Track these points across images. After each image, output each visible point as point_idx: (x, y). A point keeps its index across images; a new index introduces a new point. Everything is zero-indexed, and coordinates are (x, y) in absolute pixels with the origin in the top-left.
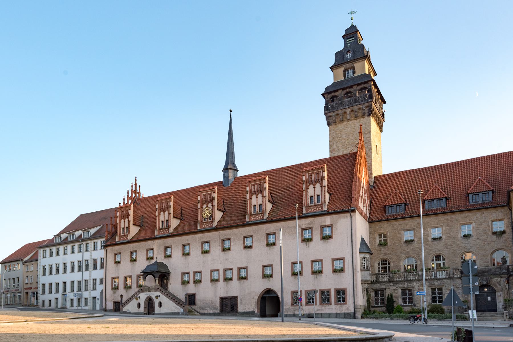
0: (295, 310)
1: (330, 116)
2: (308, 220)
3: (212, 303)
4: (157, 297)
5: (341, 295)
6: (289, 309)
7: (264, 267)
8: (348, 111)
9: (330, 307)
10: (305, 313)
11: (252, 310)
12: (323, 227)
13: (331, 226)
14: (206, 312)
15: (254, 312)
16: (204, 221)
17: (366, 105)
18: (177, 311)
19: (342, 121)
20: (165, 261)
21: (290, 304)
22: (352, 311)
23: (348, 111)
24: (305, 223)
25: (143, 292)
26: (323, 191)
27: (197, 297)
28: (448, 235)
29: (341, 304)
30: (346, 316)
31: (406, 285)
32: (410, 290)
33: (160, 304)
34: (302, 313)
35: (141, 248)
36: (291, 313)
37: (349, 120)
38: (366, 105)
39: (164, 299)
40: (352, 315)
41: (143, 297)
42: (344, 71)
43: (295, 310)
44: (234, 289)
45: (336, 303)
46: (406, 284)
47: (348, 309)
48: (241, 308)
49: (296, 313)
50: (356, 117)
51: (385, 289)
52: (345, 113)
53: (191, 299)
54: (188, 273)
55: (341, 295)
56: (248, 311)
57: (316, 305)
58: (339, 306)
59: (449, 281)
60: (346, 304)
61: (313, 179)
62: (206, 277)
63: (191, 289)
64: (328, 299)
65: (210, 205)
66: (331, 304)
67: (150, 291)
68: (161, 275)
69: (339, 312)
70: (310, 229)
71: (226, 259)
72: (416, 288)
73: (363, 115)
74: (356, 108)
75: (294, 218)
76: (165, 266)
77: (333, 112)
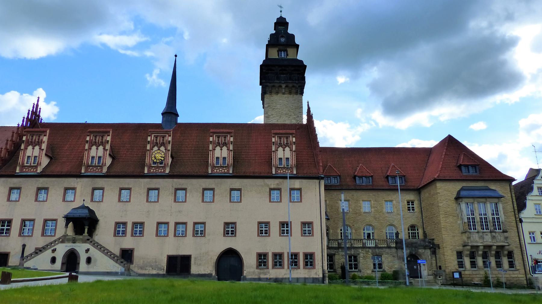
0: (260, 273)
1: (267, 86)
2: (277, 181)
3: (156, 262)
4: (87, 251)
5: (309, 259)
6: (254, 272)
7: (227, 224)
8: (284, 86)
9: (299, 271)
10: (271, 277)
11: (209, 272)
12: (292, 189)
13: (300, 189)
14: (146, 272)
15: (212, 274)
16: (153, 165)
17: (299, 85)
18: (114, 270)
19: (277, 93)
20: (92, 206)
21: (255, 266)
22: (321, 276)
23: (284, 86)
24: (273, 183)
25: (63, 242)
26: (229, 155)
27: (136, 254)
28: (376, 209)
29: (309, 269)
30: (315, 280)
31: (353, 252)
32: (355, 257)
33: (89, 260)
34: (268, 276)
35: (57, 186)
36: (256, 277)
37: (284, 94)
38: (299, 85)
39: (94, 253)
40: (321, 279)
41: (62, 249)
42: (278, 51)
43: (260, 273)
44: (185, 246)
45: (304, 268)
46: (353, 250)
47: (316, 274)
48: (194, 269)
49: (262, 276)
50: (290, 93)
51: (335, 254)
52: (281, 86)
53: (127, 256)
54: (125, 224)
55: (309, 259)
56: (203, 272)
57: (283, 268)
58: (307, 270)
59: (388, 250)
60: (315, 268)
61: (220, 141)
62: (150, 229)
63: (128, 242)
64: (296, 262)
65: (162, 148)
66: (299, 268)
67: (74, 243)
68: (84, 223)
69: (307, 276)
70: (279, 189)
71: (180, 212)
72: (361, 255)
73: (296, 93)
74: (290, 85)
75: (285, 178)
76: (92, 212)
77: (270, 83)
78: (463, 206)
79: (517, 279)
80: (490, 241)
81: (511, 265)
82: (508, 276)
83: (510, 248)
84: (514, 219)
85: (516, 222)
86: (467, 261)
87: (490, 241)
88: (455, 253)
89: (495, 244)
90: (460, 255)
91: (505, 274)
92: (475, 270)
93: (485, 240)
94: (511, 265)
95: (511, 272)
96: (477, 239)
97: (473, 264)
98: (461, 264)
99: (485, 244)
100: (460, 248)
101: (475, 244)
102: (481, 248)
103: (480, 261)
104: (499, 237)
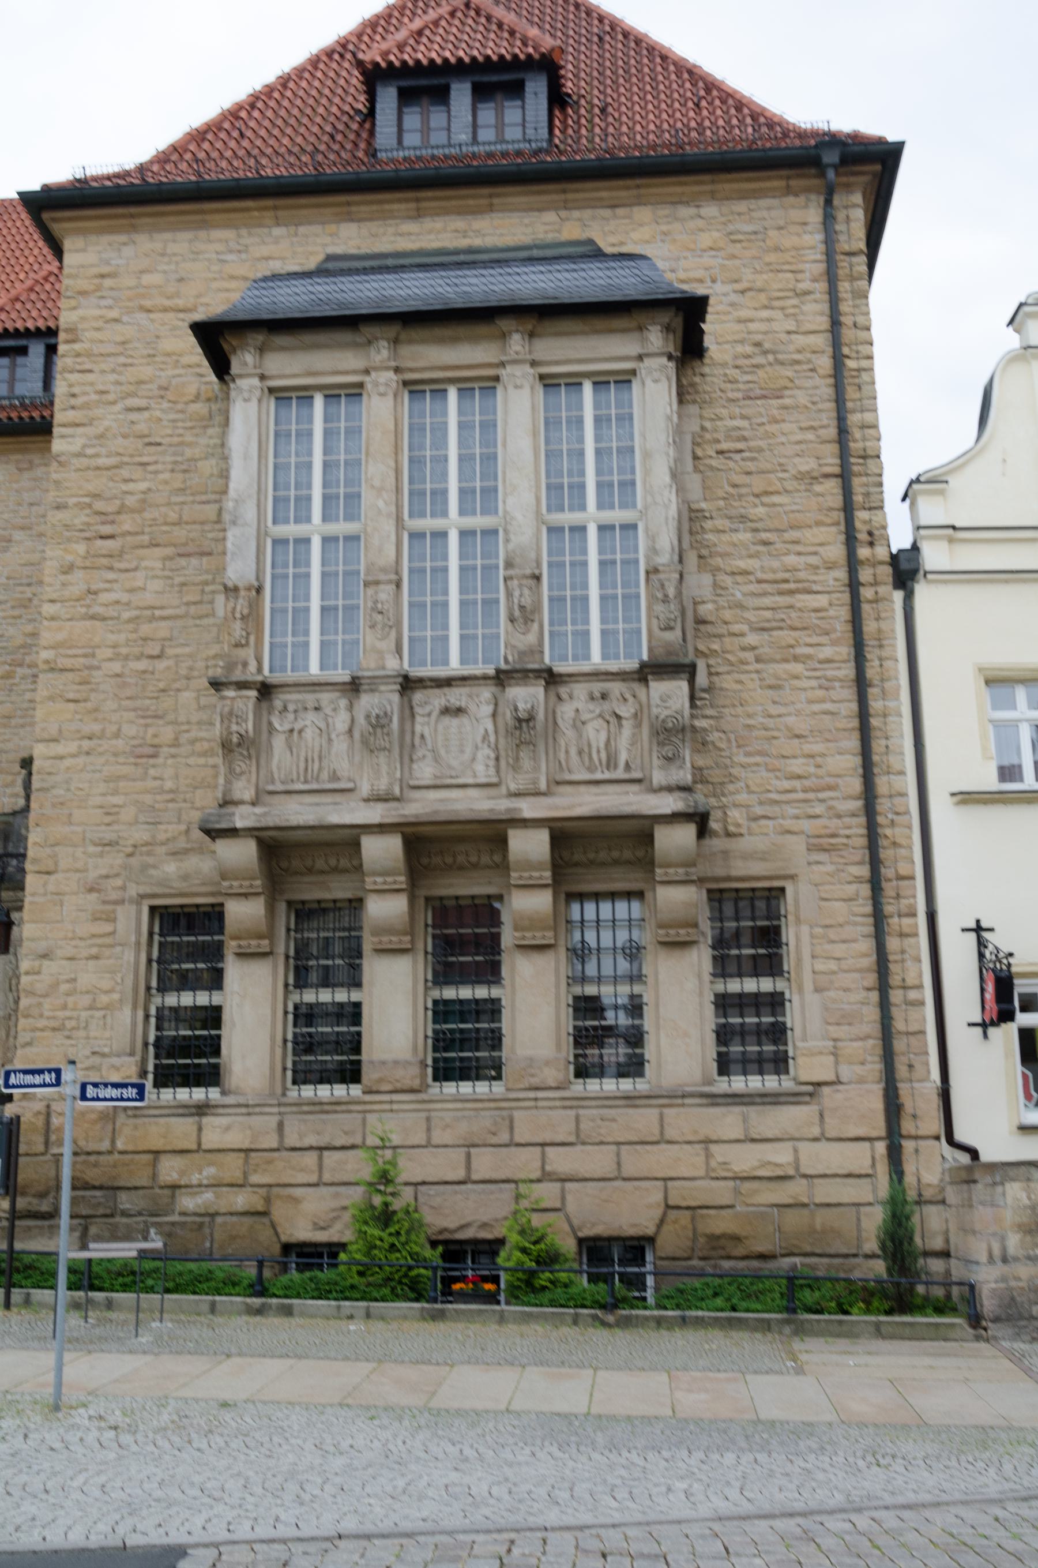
78: (247, 414)
79: (796, 1190)
80: (483, 772)
81: (752, 1036)
82: (686, 1161)
83: (747, 860)
84: (837, 551)
85: (854, 586)
86: (252, 1007)
87: (483, 772)
88: (132, 924)
89: (528, 808)
90: (187, 937)
91: (675, 1145)
92: (318, 1106)
93: (425, 771)
94: (752, 1036)
95: (728, 1122)
96: (341, 757)
97: (326, 1049)
98: (188, 1054)
99: (420, 807)
100: (186, 874)
101: (298, 813)
102: (382, 851)
103: (394, 1001)
104: (596, 734)
